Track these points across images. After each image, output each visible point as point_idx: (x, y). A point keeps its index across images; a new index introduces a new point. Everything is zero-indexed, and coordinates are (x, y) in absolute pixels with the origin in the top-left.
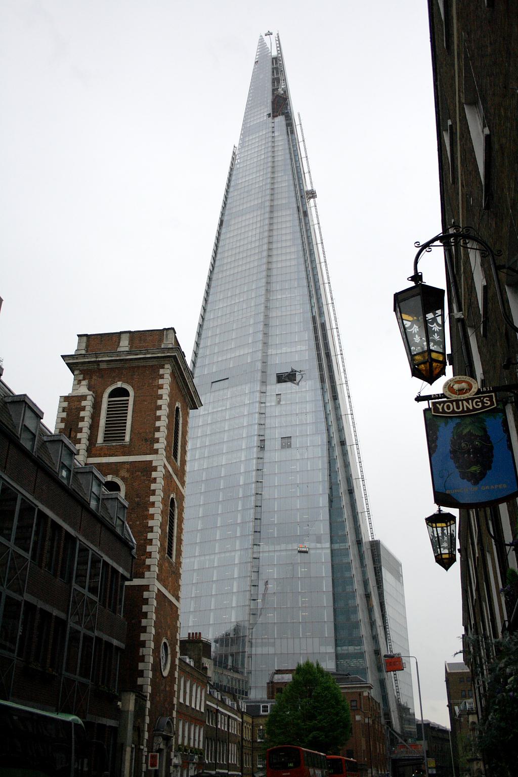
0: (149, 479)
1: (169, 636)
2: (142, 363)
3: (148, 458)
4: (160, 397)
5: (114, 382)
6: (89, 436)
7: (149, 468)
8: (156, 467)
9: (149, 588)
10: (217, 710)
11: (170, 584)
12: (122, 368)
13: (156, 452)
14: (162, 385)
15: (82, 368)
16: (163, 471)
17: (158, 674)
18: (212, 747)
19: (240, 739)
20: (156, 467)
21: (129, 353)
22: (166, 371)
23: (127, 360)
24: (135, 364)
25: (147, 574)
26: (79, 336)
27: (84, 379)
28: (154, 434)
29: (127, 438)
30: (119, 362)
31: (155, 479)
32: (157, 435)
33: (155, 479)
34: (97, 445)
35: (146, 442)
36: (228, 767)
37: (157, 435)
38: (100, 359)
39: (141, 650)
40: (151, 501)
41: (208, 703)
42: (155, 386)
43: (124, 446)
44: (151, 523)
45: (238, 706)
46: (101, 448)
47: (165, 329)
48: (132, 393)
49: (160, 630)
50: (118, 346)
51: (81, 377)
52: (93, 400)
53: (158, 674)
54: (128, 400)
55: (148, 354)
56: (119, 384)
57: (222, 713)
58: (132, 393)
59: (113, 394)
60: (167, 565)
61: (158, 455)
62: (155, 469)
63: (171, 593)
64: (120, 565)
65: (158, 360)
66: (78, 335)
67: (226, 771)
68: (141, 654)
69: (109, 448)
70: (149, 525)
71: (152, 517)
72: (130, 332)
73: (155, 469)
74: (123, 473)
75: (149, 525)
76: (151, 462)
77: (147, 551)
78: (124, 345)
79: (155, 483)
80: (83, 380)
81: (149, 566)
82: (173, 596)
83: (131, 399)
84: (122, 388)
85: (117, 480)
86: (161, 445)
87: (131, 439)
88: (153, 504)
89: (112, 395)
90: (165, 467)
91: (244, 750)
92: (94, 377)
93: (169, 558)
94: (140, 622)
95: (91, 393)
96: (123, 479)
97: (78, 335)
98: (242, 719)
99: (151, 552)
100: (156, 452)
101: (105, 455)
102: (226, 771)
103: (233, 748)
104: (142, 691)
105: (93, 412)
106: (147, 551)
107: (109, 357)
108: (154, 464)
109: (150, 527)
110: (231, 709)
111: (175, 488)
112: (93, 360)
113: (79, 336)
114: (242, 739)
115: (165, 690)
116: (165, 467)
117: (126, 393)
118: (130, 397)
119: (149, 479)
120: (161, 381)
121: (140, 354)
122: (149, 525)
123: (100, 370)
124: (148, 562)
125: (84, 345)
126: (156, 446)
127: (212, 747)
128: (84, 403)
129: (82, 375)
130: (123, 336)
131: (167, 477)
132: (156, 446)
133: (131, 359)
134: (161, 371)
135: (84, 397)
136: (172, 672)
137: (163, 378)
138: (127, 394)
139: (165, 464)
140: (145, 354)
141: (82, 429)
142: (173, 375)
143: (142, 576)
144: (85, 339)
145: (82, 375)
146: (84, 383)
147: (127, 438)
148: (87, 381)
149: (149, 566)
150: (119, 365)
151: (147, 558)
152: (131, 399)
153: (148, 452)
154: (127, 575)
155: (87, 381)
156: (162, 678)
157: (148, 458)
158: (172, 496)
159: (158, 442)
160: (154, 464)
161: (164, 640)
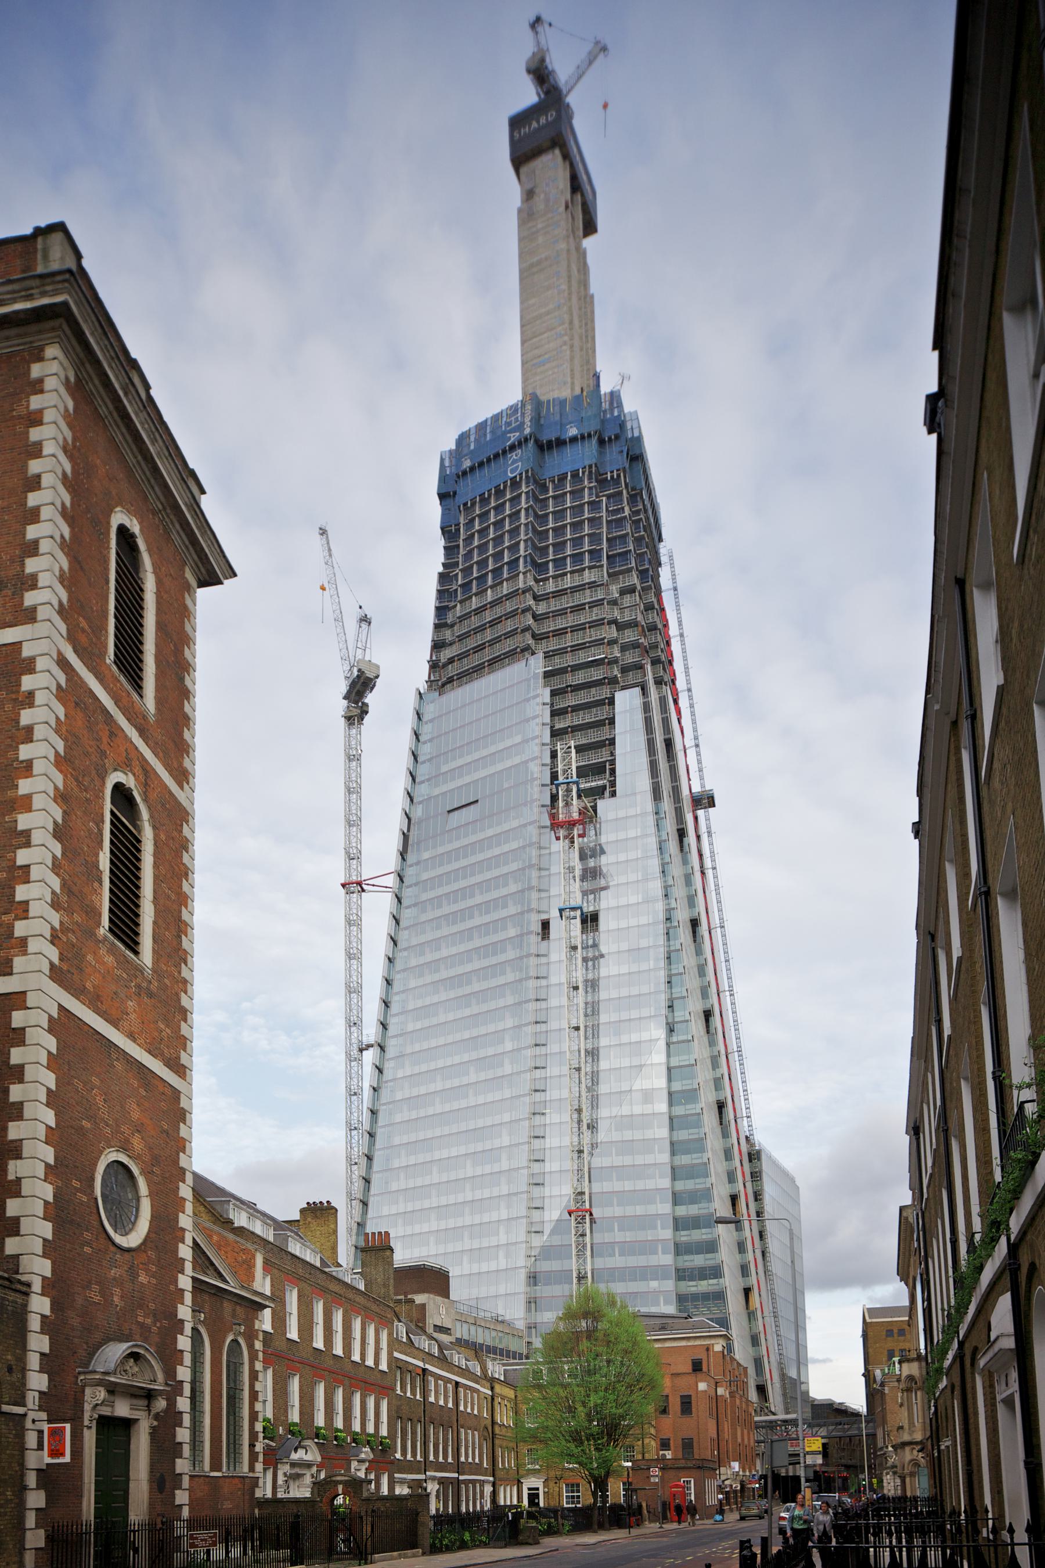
0: (14, 696)
4: (36, 451)
8: (32, 660)
14: (40, 412)
16: (62, 679)
18: (414, 1433)
19: (489, 1423)
20: (32, 660)
31: (31, 694)
33: (31, 694)
36: (459, 1468)
42: (20, 417)
44: (24, 821)
45: (484, 1369)
61: (36, 624)
67: (456, 1475)
71: (26, 804)
73: (29, 665)
76: (17, 646)
77: (18, 898)
79: (31, 705)
81: (23, 942)
86: (47, 595)
88: (27, 768)
90: (63, 663)
91: (497, 1442)
98: (492, 1389)
99: (27, 902)
102: (456, 1475)
103: (470, 1438)
104: (17, 1273)
106: (18, 898)
108: (26, 652)
109: (23, 832)
110: (465, 1372)
114: (493, 1423)
116: (63, 663)
119: (14, 696)
124: (20, 928)
127: (414, 1433)
131: (73, 693)
137: (42, 391)
139: (59, 653)
149: (23, 942)
151: (18, 918)
153: (8, 618)
159: (34, 586)
160: (26, 652)
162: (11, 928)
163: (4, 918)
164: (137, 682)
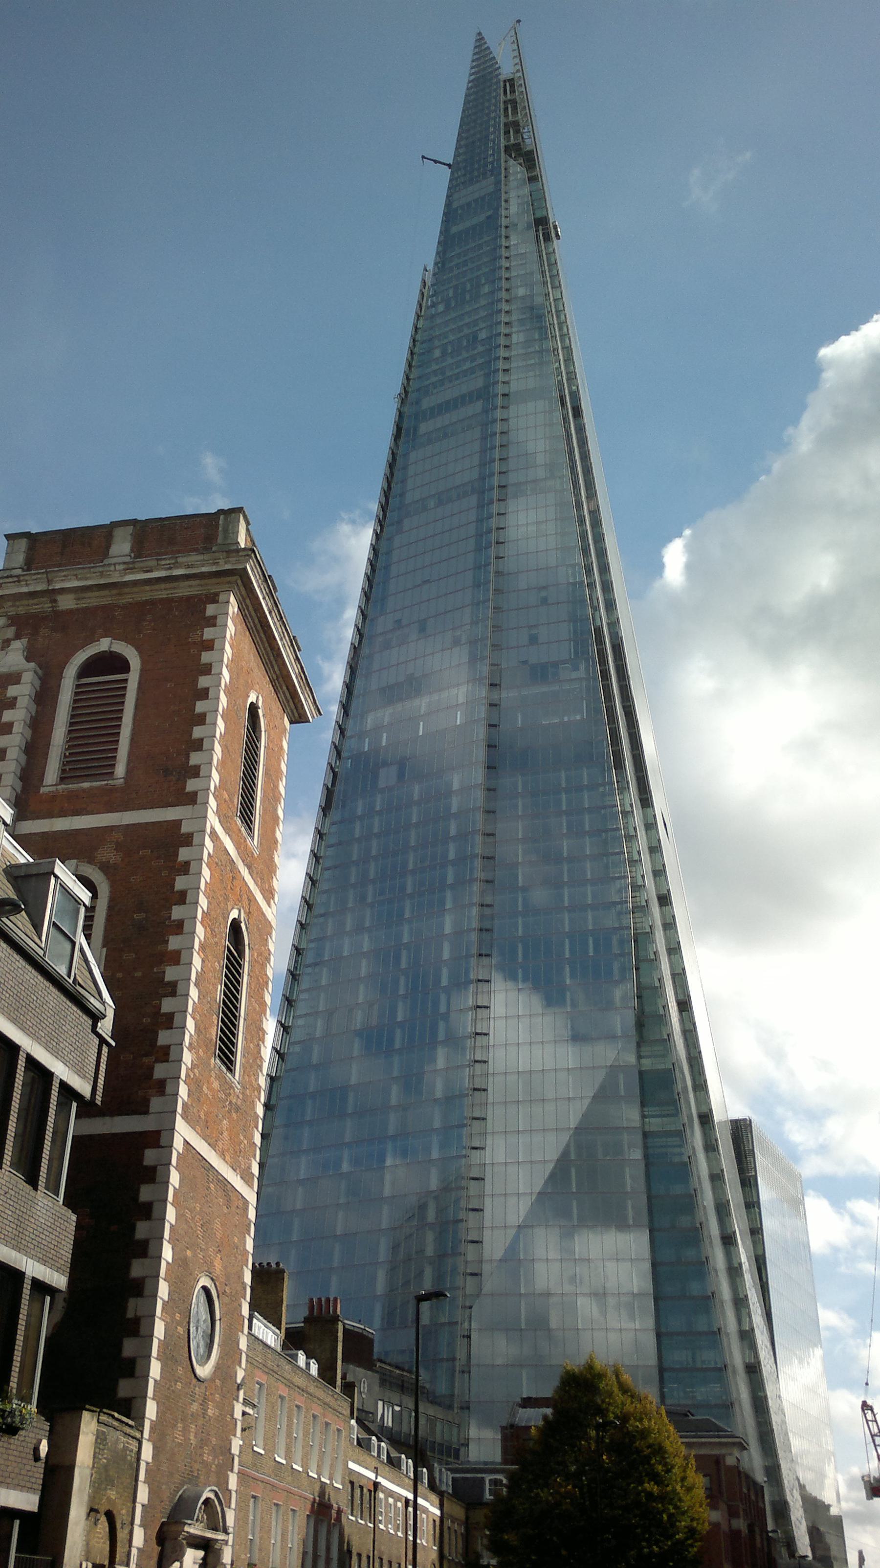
1: (218, 1271)
2: (162, 593)
5: (92, 639)
6: (22, 769)
9: (159, 1140)
10: (376, 1485)
11: (225, 1134)
15: (12, 612)
17: (180, 1371)
21: (130, 568)
23: (125, 584)
25: (156, 1103)
26: (8, 537)
27: (18, 637)
28: (188, 758)
29: (120, 770)
30: (106, 592)
34: (43, 790)
38: (58, 586)
39: (132, 1303)
40: (173, 918)
41: (352, 1465)
43: (112, 790)
46: (53, 798)
47: (221, 512)
48: (135, 662)
49: (189, 1253)
50: (106, 555)
52: (38, 683)
53: (180, 1371)
54: (126, 681)
55: (177, 568)
56: (104, 644)
57: (390, 1493)
58: (135, 662)
59: (89, 669)
60: (216, 1085)
63: (228, 1158)
64: (56, 1053)
65: (203, 582)
66: (5, 535)
68: (130, 1314)
69: (72, 796)
70: (167, 979)
72: (134, 522)
73: (187, 840)
74: (108, 854)
75: (168, 978)
76: (178, 823)
80: (14, 640)
82: (235, 1170)
83: (133, 679)
84: (111, 652)
85: (90, 871)
87: (129, 771)
89: (86, 670)
92: (44, 631)
93: (224, 1068)
94: (133, 1228)
95: (32, 664)
96: (105, 868)
97: (5, 535)
98: (441, 1508)
101: (63, 814)
105: (37, 711)
107: (81, 579)
108: (184, 829)
111: (245, 897)
112: (39, 588)
113: (8, 537)
115: (204, 1414)
117: (120, 664)
118: (131, 673)
121: (158, 570)
122: (167, 979)
123: (58, 614)
125: (20, 558)
126: (192, 785)
128: (12, 691)
129: (13, 629)
130: (119, 533)
132: (192, 785)
133: (135, 583)
134: (210, 610)
136: (224, 1371)
138: (123, 666)
140: (170, 568)
141: (5, 752)
143: (143, 1109)
144: (23, 544)
145: (13, 629)
147: (120, 770)
148: (25, 641)
152: (133, 679)
154: (84, 1087)
155: (25, 641)
156: (194, 1381)
158: (234, 914)
160: (184, 829)
161: (204, 1281)
162: (151, 1069)
163: (146, 1060)
164: (250, 829)
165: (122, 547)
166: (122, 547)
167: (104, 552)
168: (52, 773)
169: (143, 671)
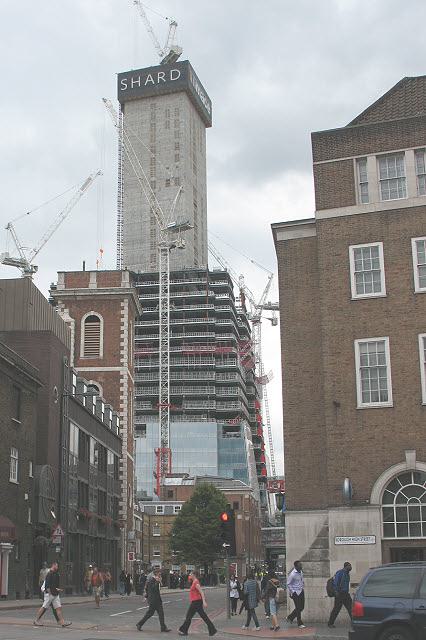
3: (117, 369)
7: (117, 376)
12: (92, 301)
13: (122, 365)
22: (125, 304)
24: (102, 298)
29: (101, 354)
32: (122, 352)
35: (114, 357)
37: (122, 352)
43: (99, 360)
46: (83, 361)
48: (102, 320)
51: (63, 306)
56: (92, 313)
58: (102, 320)
62: (122, 377)
73: (122, 377)
78: (93, 284)
96: (100, 383)
100: (122, 365)
120: (122, 312)
125: (63, 280)
135: (69, 324)
138: (99, 321)
142: (129, 306)
146: (66, 310)
147: (101, 354)
150: (91, 298)
157: (117, 369)
165: (93, 279)
166: (93, 279)
167: (87, 281)
168: (82, 355)
169: (104, 323)
